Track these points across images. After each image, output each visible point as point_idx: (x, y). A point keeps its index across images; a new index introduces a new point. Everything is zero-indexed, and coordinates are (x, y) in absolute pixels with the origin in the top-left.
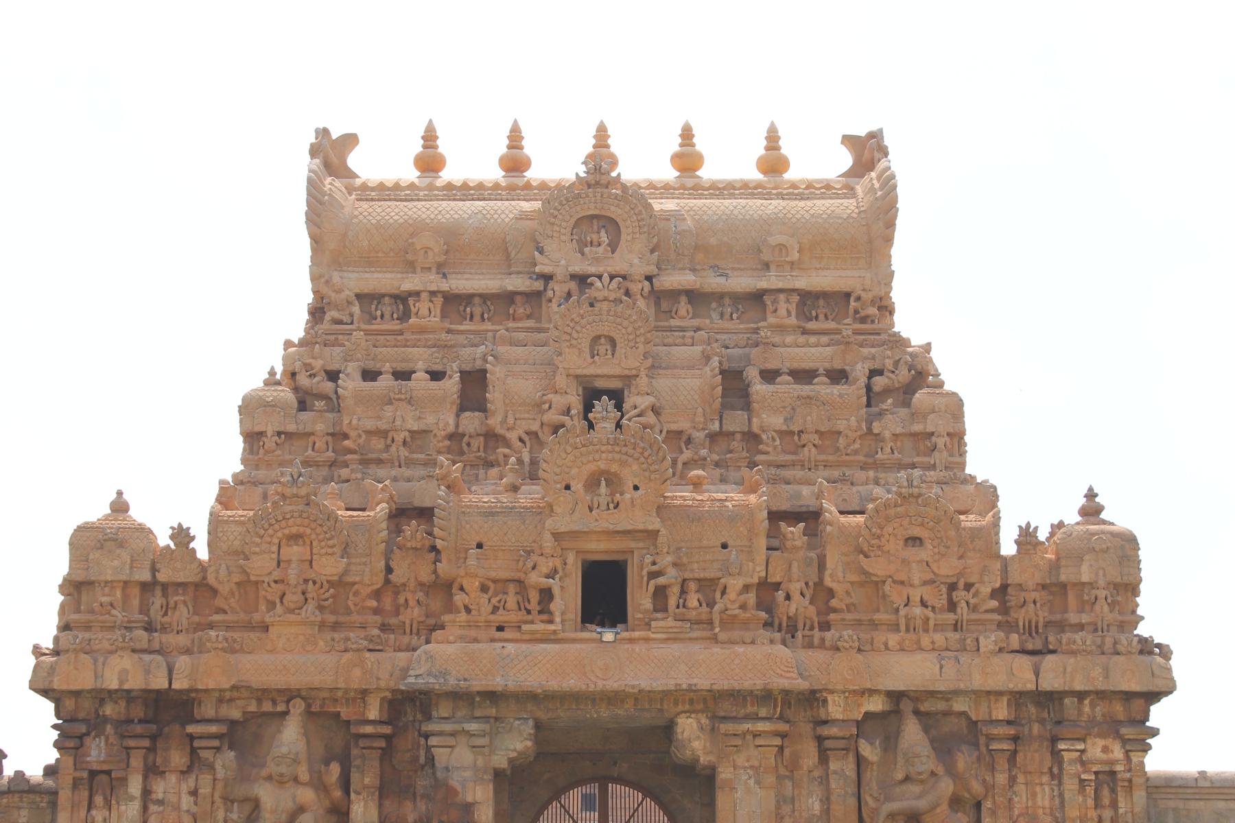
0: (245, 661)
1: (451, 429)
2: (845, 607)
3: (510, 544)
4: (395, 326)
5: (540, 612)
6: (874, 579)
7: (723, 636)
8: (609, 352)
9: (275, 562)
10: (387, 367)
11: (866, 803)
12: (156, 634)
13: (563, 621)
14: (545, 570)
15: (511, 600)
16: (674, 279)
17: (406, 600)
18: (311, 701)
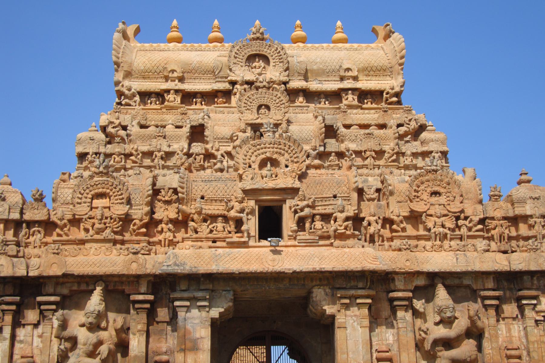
0: (70, 260)
1: (185, 151)
2: (400, 229)
3: (219, 196)
4: (158, 107)
5: (236, 233)
6: (416, 214)
8: (267, 112)
9: (89, 208)
10: (153, 123)
11: (420, 335)
12: (21, 248)
13: (249, 236)
16: (297, 83)
17: (162, 229)
18: (108, 283)
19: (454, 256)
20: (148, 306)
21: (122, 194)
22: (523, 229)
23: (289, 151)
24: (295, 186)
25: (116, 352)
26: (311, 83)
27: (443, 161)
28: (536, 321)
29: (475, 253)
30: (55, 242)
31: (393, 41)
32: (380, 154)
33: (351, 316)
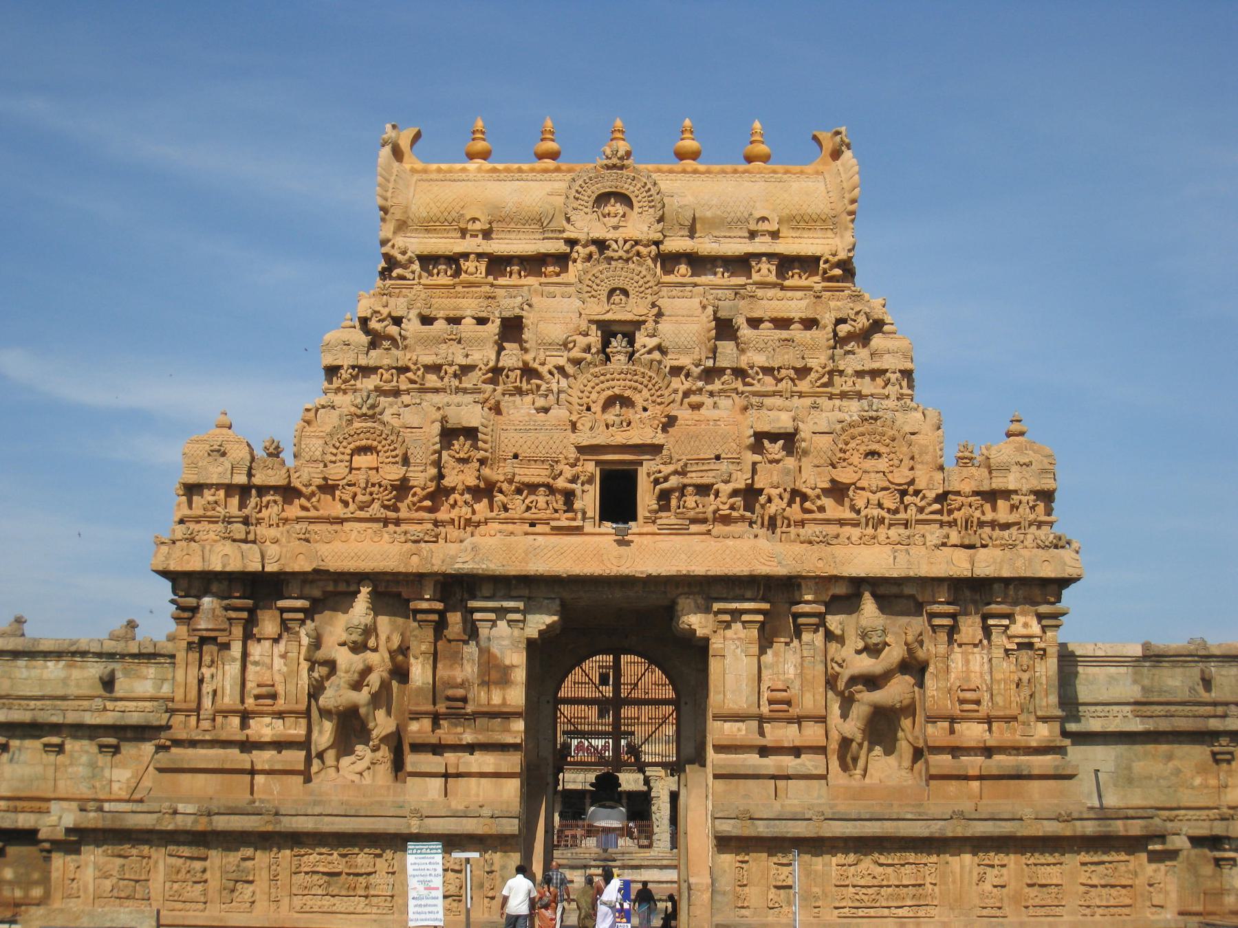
0: (323, 549)
1: (492, 364)
6: (840, 486)
7: (714, 532)
9: (348, 470)
10: (441, 314)
11: (832, 668)
12: (252, 528)
13: (584, 519)
14: (569, 476)
15: (542, 504)
16: (677, 243)
17: (456, 502)
19: (890, 553)
20: (435, 617)
21: (395, 449)
22: (1003, 512)
23: (650, 386)
24: (656, 441)
25: (391, 679)
26: (701, 240)
27: (904, 384)
28: (1006, 651)
29: (923, 548)
30: (298, 520)
31: (841, 169)
32: (803, 372)
33: (733, 640)
